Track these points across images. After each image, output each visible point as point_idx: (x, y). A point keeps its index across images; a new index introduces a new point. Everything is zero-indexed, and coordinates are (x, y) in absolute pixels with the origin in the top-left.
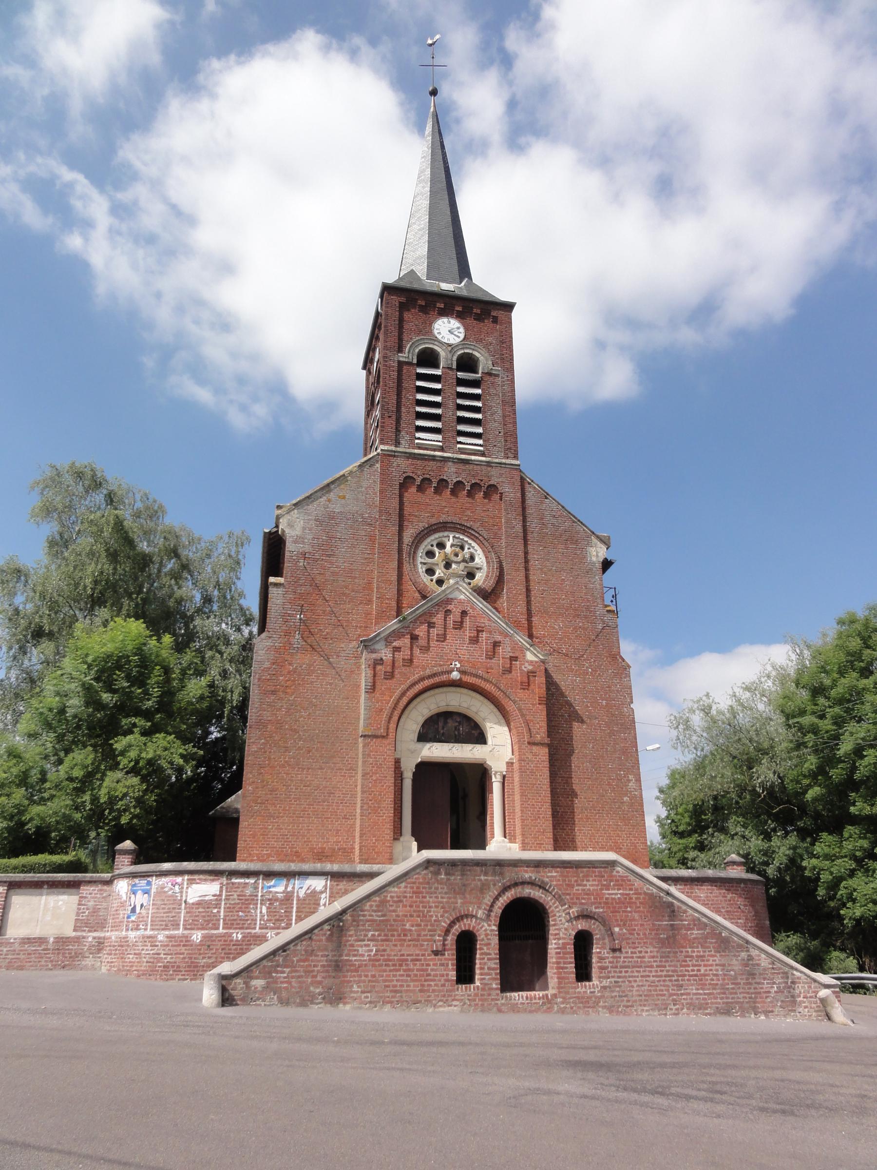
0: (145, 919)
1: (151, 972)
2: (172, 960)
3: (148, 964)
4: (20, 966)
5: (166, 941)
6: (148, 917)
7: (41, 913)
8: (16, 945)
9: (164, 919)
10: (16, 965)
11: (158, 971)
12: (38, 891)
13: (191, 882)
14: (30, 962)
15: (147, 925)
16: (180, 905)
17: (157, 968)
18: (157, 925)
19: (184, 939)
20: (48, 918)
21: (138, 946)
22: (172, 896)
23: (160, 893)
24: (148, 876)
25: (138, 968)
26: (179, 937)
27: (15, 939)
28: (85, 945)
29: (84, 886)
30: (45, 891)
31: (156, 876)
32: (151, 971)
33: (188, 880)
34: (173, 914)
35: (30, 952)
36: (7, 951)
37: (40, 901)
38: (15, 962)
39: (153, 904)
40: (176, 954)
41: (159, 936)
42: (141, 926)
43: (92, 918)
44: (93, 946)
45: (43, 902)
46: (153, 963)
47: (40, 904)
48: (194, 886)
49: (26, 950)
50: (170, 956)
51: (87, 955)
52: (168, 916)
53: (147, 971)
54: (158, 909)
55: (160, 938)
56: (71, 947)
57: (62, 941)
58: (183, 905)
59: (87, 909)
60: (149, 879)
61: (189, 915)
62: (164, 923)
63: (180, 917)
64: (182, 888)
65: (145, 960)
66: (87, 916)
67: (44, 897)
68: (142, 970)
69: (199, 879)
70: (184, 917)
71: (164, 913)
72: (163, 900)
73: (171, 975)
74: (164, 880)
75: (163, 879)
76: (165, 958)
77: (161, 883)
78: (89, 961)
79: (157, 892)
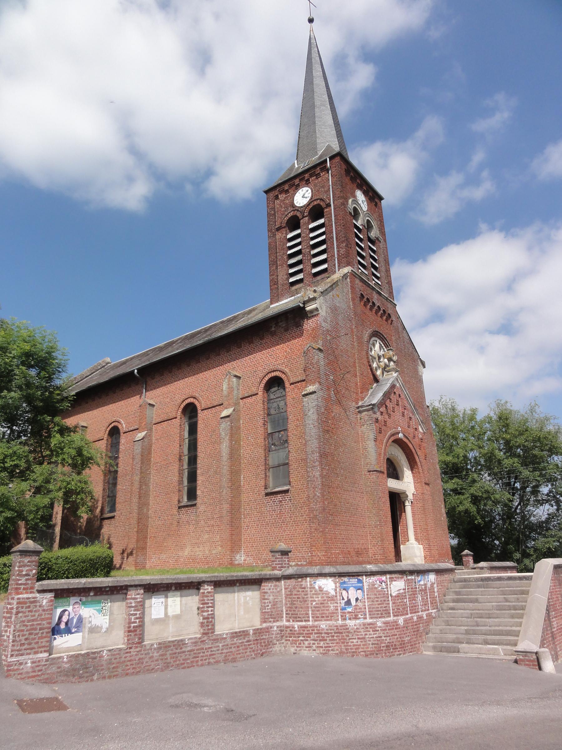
0: (363, 610)
1: (377, 652)
2: (390, 641)
3: (374, 646)
4: (233, 658)
5: (384, 626)
6: (365, 608)
7: (236, 609)
8: (228, 640)
9: (379, 609)
10: (230, 658)
11: (382, 650)
12: (231, 589)
13: (392, 579)
14: (240, 654)
15: (365, 615)
16: (388, 598)
17: (382, 648)
18: (374, 614)
19: (395, 624)
20: (242, 613)
21: (360, 632)
22: (382, 591)
23: (372, 589)
24: (358, 576)
25: (365, 650)
26: (392, 622)
27: (227, 634)
28: (273, 634)
29: (265, 582)
30: (236, 588)
31: (366, 575)
32: (377, 651)
33: (390, 578)
34: (385, 605)
35: (238, 644)
36: (223, 646)
37: (234, 597)
38: (229, 655)
39: (367, 598)
40: (392, 635)
41: (378, 623)
42: (360, 616)
43: (274, 610)
44: (278, 633)
45: (236, 598)
46: (378, 644)
47: (235, 600)
48: (394, 583)
49: (236, 644)
50: (388, 638)
51: (275, 641)
52: (382, 607)
53: (374, 651)
54: (372, 601)
55: (379, 624)
56: (264, 637)
57: (258, 632)
58: (390, 597)
59: (270, 602)
60: (360, 578)
61: (394, 605)
62: (380, 612)
63: (389, 607)
64: (387, 585)
65: (370, 643)
66: (270, 609)
67: (236, 594)
68: (368, 651)
69: (395, 577)
70: (392, 606)
71: (378, 604)
72: (375, 595)
73: (392, 652)
74: (373, 579)
75: (372, 578)
76: (386, 640)
77: (371, 581)
78: (277, 648)
79: (369, 588)
